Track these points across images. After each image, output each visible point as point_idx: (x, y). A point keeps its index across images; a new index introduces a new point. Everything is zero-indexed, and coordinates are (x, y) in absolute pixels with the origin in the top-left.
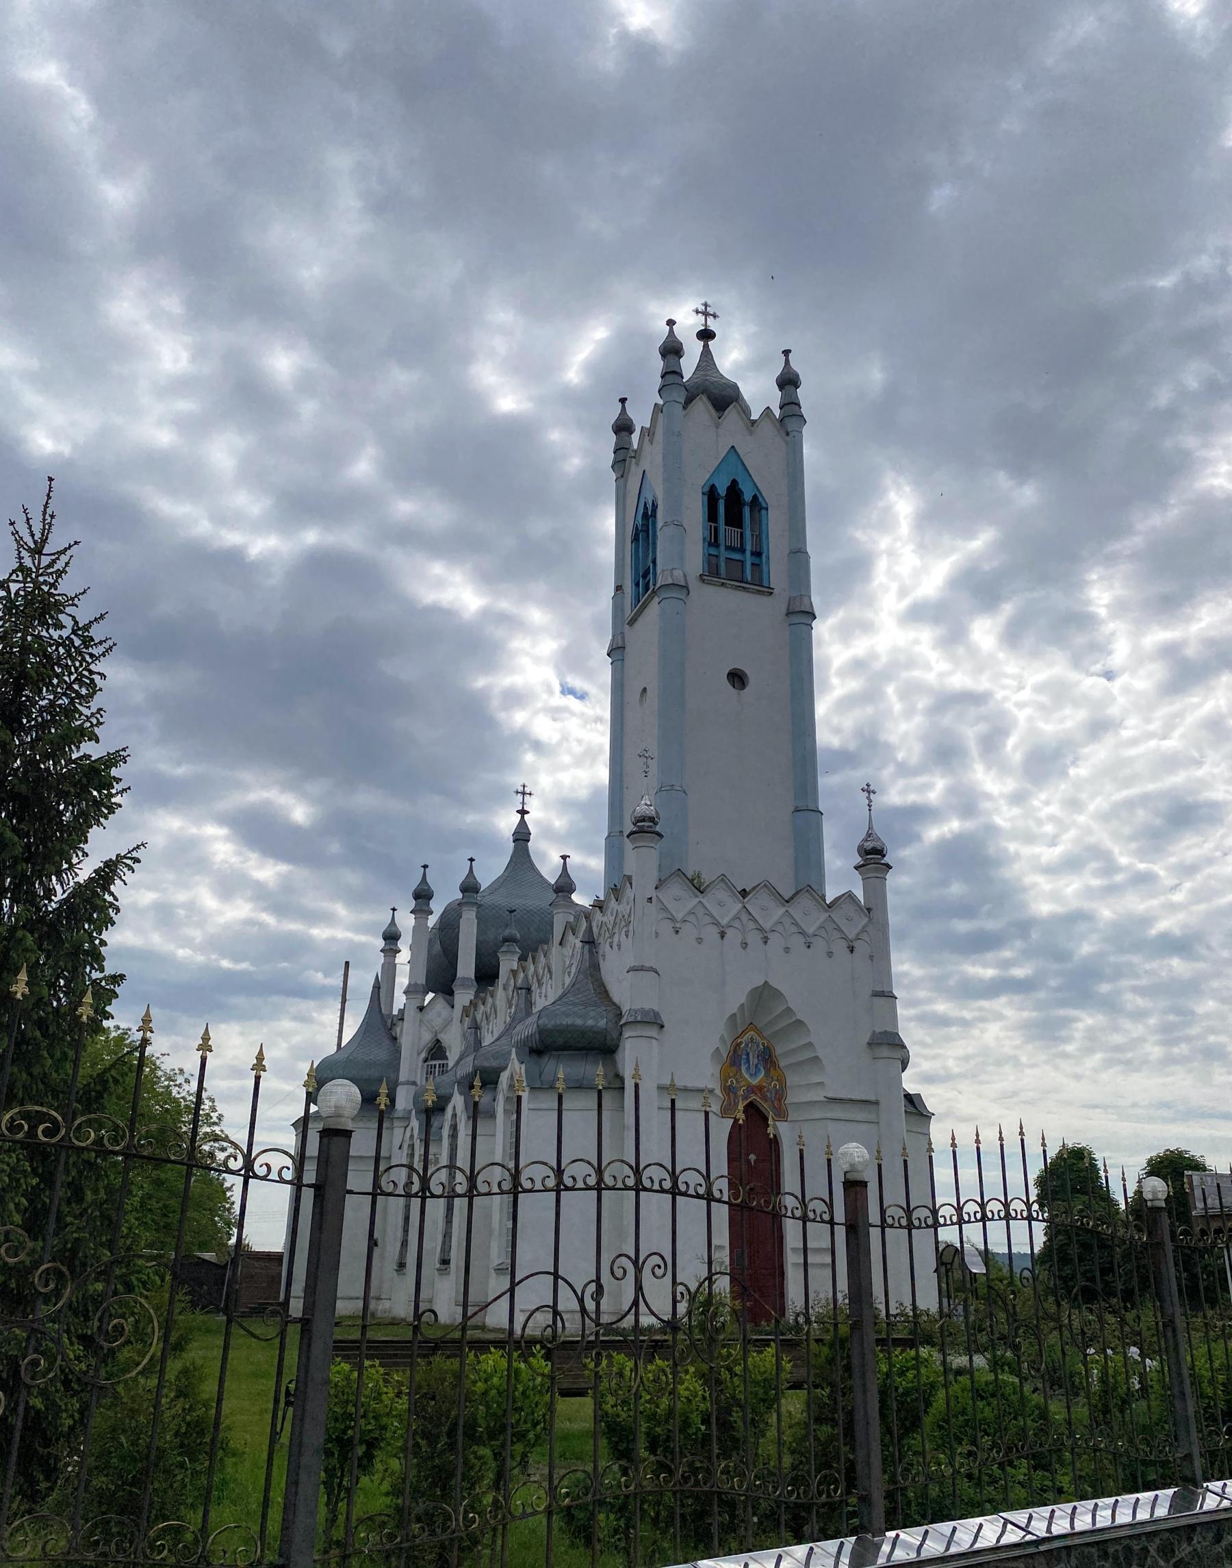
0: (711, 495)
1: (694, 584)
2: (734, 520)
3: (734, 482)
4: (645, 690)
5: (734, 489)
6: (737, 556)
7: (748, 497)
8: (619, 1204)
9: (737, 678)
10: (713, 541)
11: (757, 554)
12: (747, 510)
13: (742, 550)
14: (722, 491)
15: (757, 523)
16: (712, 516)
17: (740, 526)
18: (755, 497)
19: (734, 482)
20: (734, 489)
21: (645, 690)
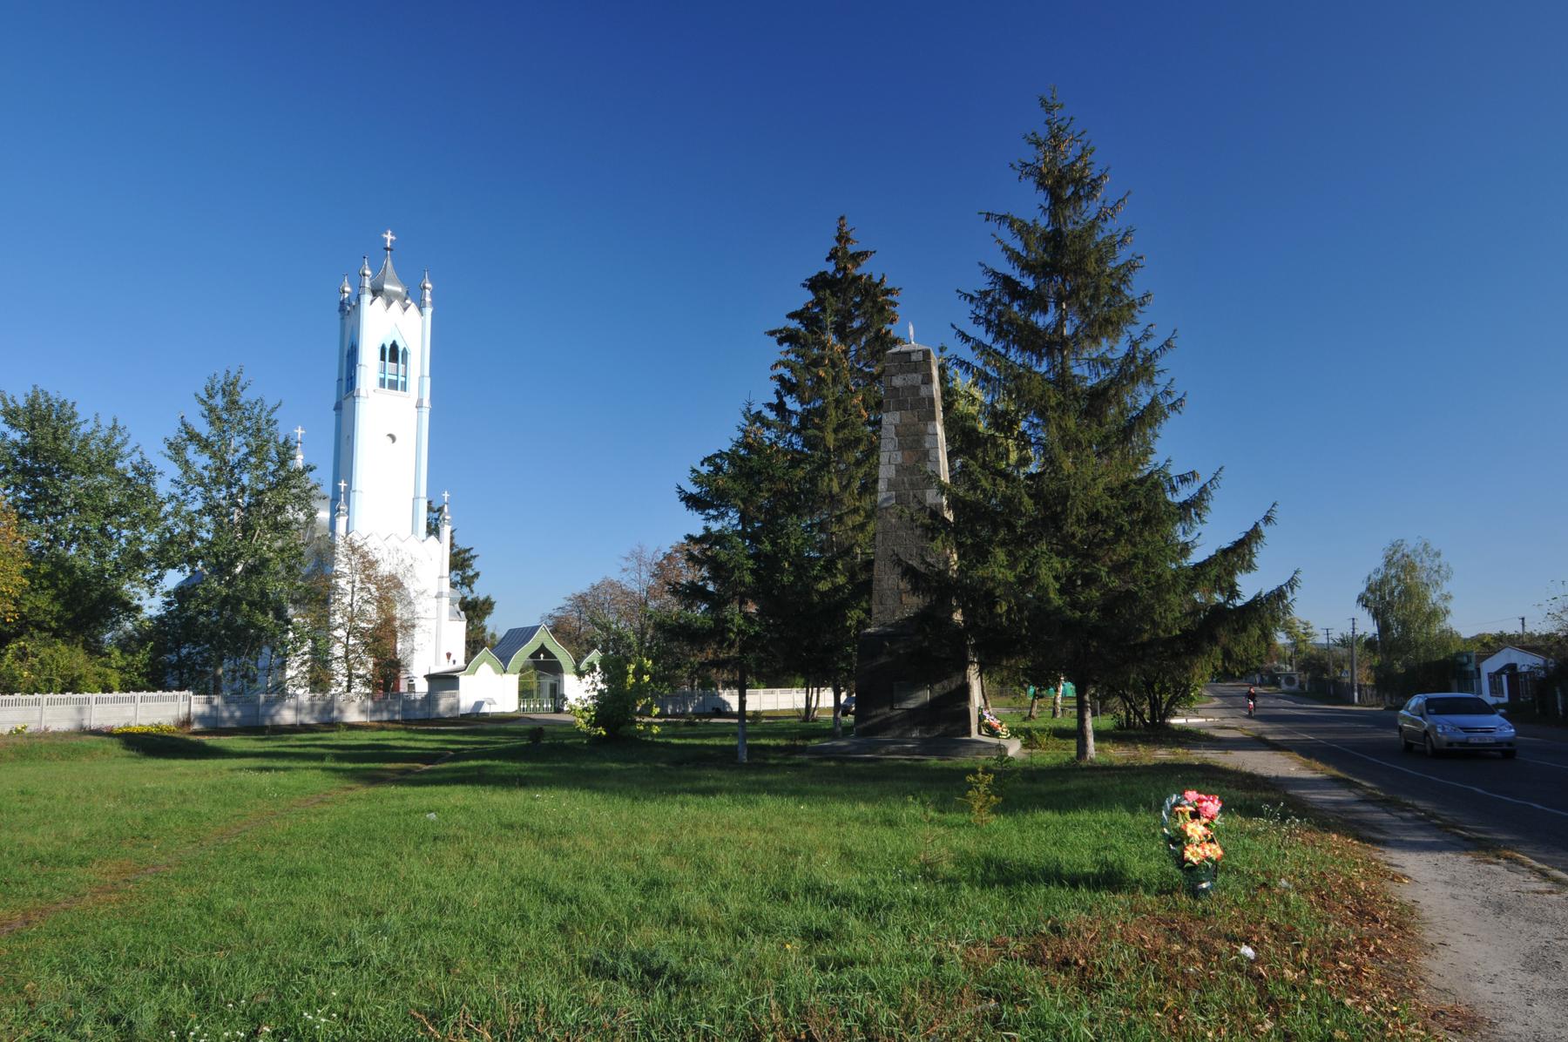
0: (383, 349)
2: (394, 358)
5: (394, 347)
7: (401, 349)
9: (393, 437)
14: (388, 347)
15: (405, 362)
16: (383, 358)
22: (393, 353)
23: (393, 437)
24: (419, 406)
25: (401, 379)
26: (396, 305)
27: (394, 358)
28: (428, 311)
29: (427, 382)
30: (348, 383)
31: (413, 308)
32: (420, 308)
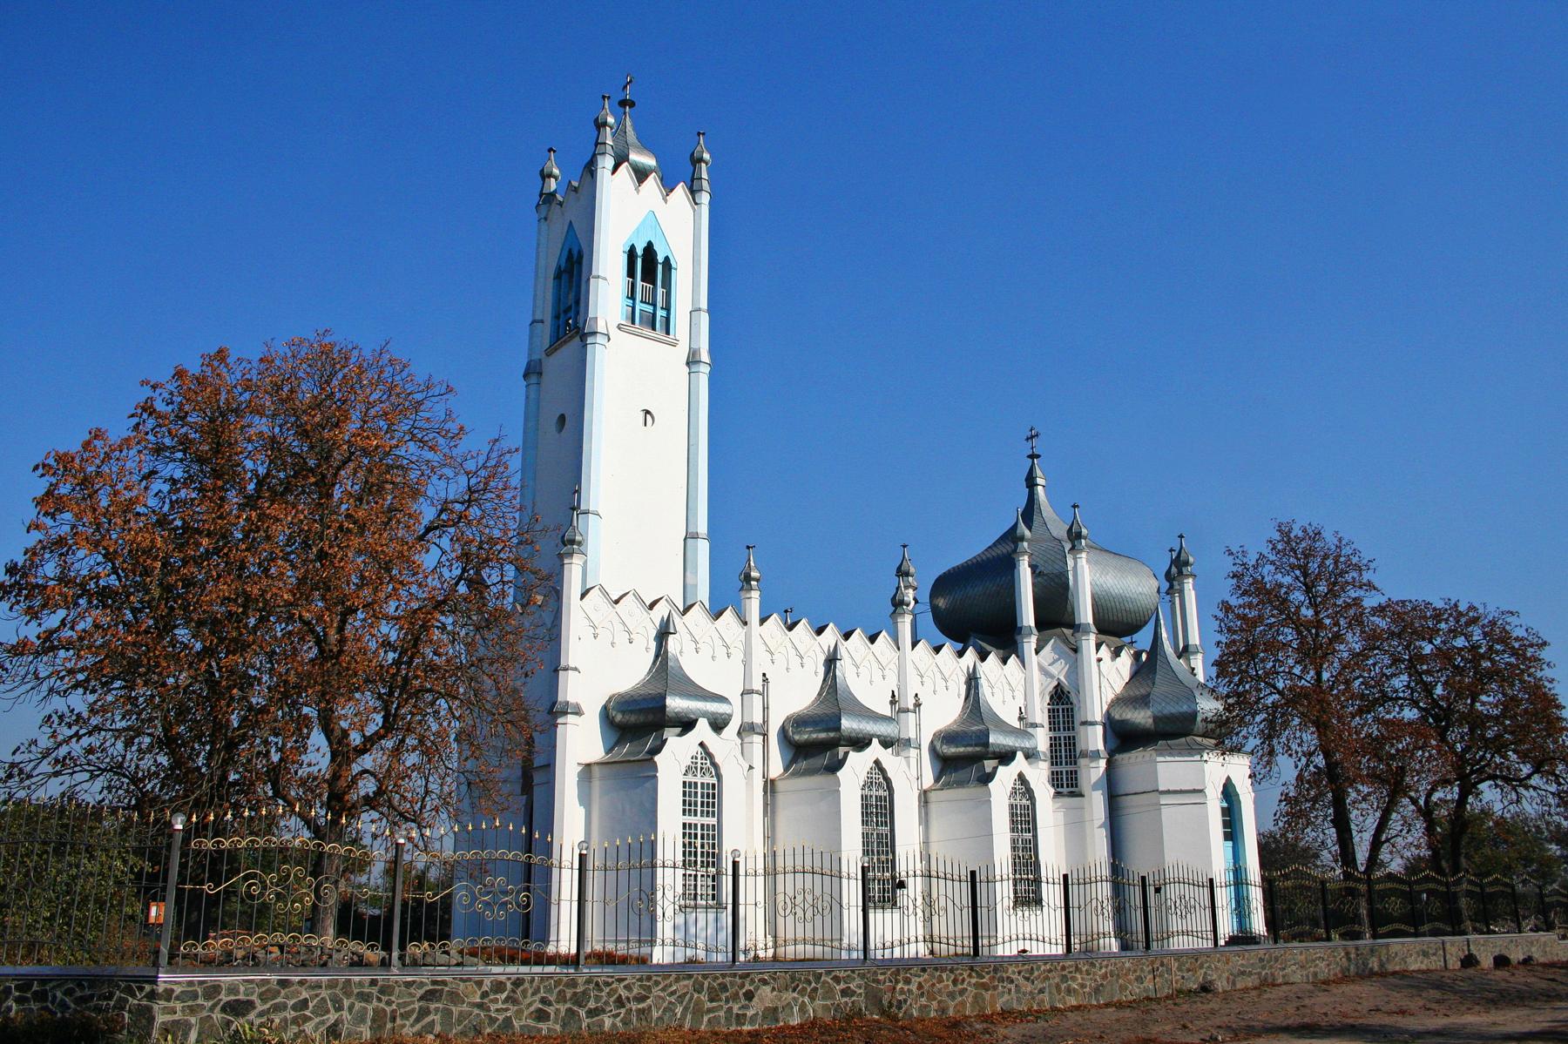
0: (631, 254)
1: (614, 332)
2: (649, 276)
3: (650, 244)
4: (562, 419)
5: (649, 250)
6: (650, 309)
7: (660, 259)
8: (799, 876)
10: (632, 296)
11: (667, 308)
12: (660, 267)
13: (654, 305)
14: (640, 252)
15: (667, 284)
16: (631, 273)
17: (654, 283)
18: (667, 259)
19: (650, 244)
20: (649, 250)
21: (562, 419)
22: (647, 266)
23: (647, 412)
24: (692, 361)
25: (660, 313)
26: (652, 182)
27: (649, 276)
28: (705, 198)
29: (704, 319)
30: (569, 323)
31: (680, 191)
32: (693, 191)
